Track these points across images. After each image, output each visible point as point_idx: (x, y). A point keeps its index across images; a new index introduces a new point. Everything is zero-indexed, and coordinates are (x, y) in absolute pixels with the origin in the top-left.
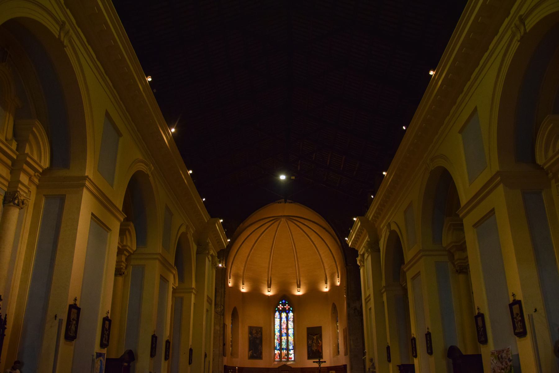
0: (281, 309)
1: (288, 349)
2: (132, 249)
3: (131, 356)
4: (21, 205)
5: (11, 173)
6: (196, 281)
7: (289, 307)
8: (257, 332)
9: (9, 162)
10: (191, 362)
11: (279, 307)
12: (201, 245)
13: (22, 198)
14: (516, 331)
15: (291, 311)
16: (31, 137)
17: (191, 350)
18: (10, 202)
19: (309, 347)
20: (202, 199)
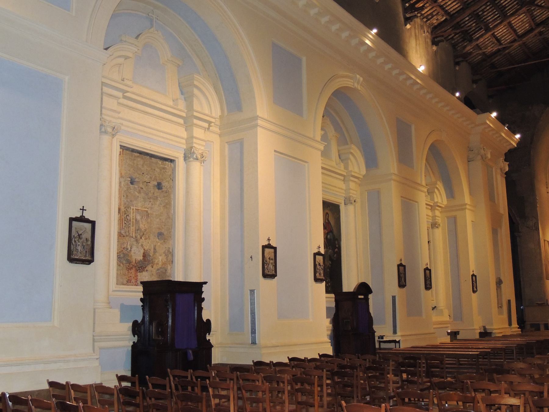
4: (202, 159)
5: (186, 130)
6: (471, 194)
9: (181, 121)
10: (475, 289)
12: (473, 150)
13: (200, 152)
16: (196, 91)
18: (189, 158)
20: (454, 95)
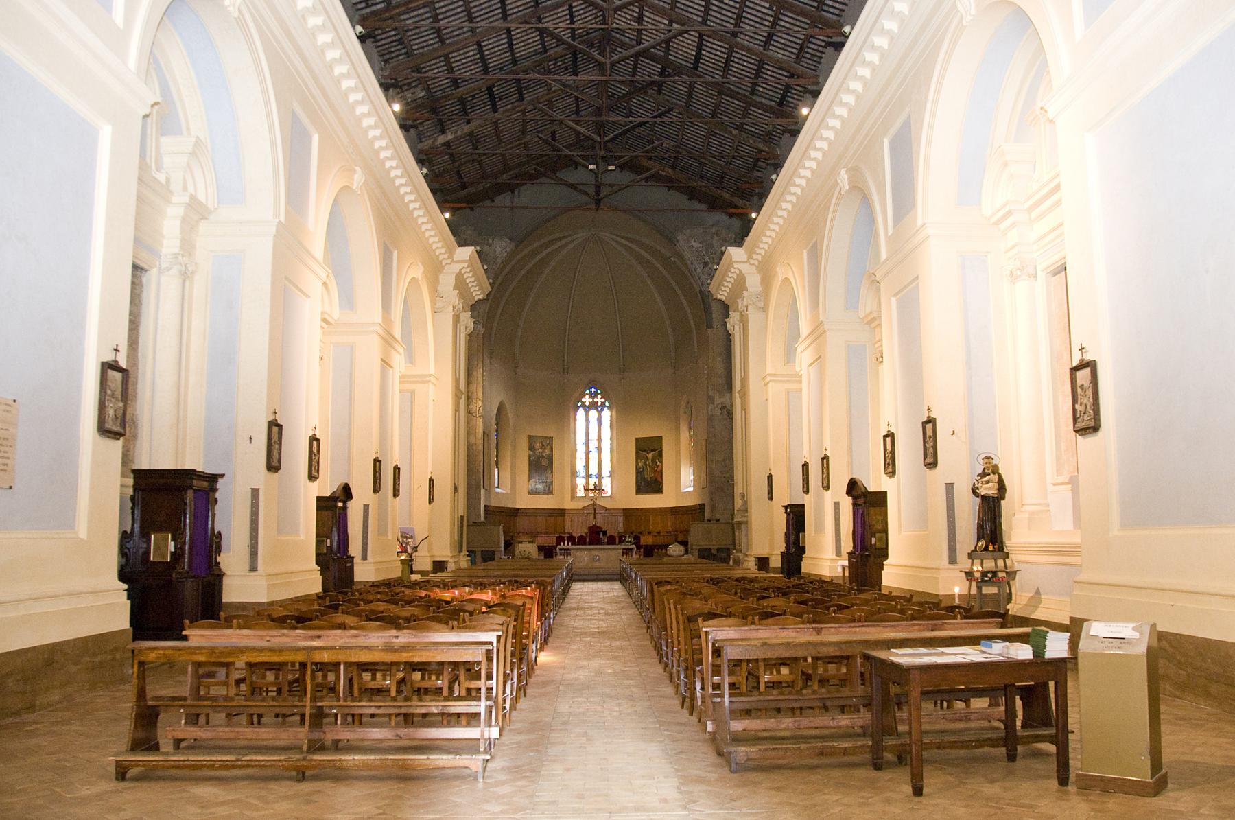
0: (587, 404)
1: (599, 476)
2: (333, 318)
3: (346, 492)
7: (603, 400)
8: (543, 445)
11: (583, 400)
14: (926, 461)
15: (606, 409)
17: (431, 480)
19: (639, 472)
